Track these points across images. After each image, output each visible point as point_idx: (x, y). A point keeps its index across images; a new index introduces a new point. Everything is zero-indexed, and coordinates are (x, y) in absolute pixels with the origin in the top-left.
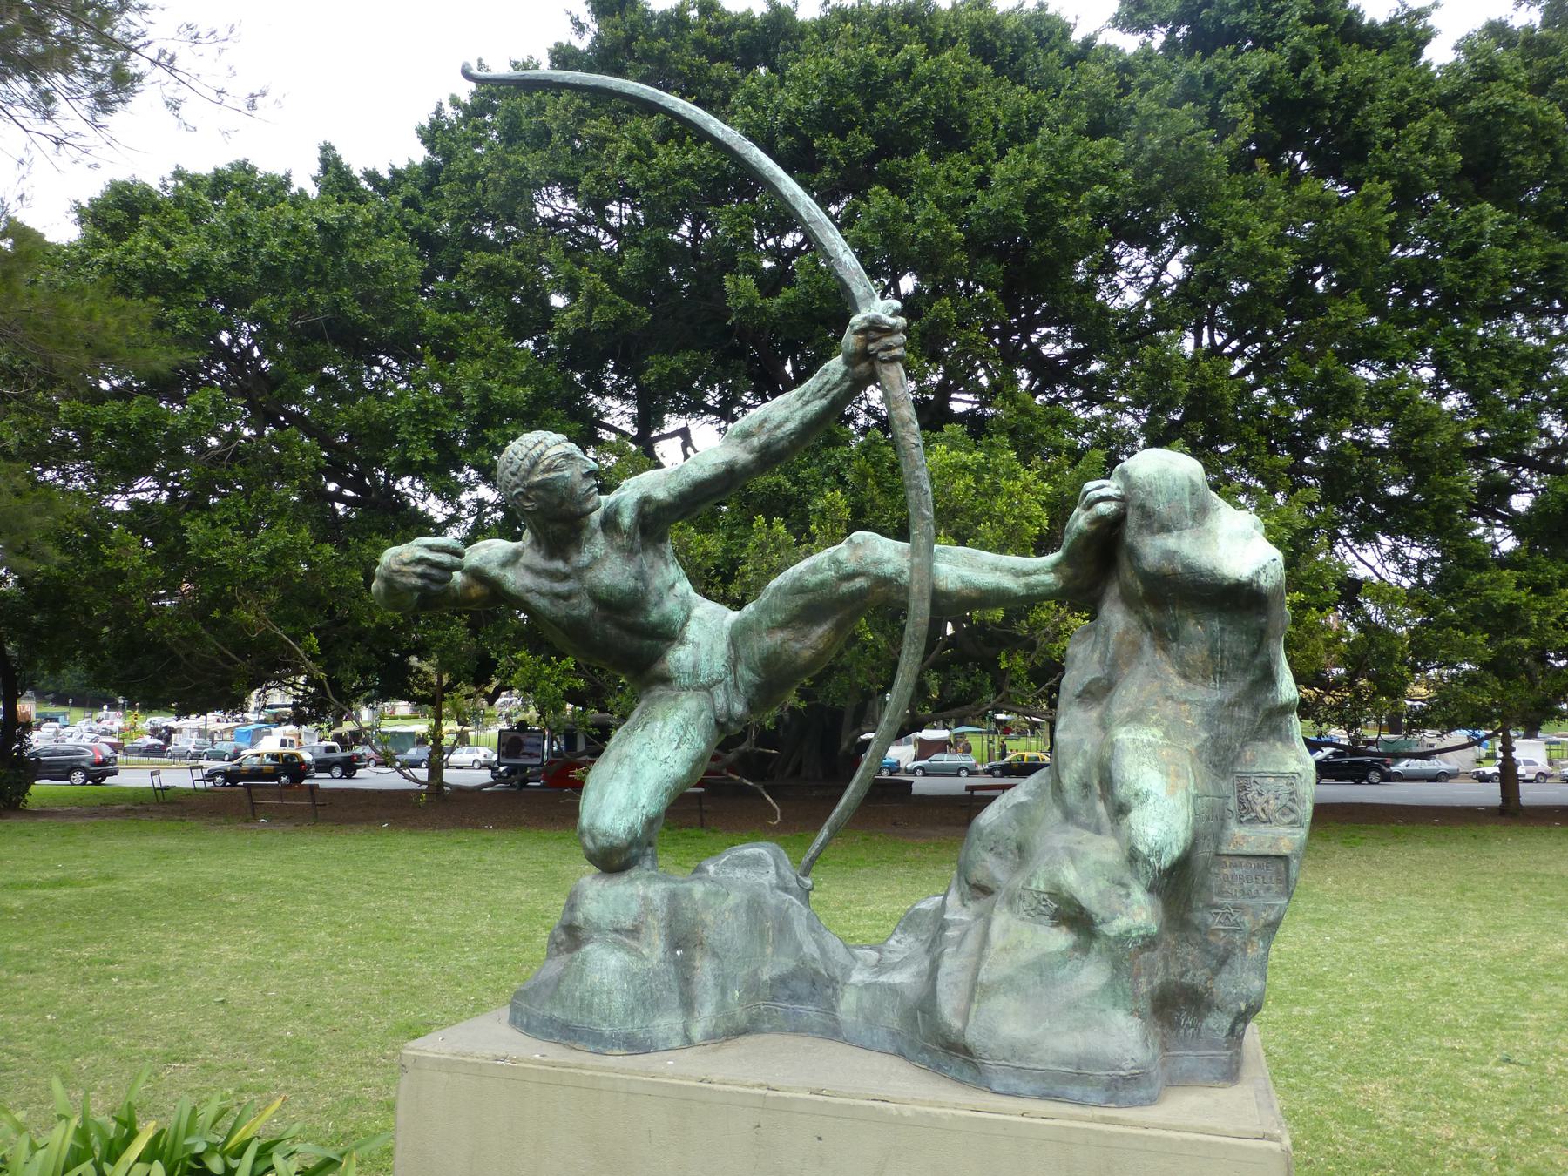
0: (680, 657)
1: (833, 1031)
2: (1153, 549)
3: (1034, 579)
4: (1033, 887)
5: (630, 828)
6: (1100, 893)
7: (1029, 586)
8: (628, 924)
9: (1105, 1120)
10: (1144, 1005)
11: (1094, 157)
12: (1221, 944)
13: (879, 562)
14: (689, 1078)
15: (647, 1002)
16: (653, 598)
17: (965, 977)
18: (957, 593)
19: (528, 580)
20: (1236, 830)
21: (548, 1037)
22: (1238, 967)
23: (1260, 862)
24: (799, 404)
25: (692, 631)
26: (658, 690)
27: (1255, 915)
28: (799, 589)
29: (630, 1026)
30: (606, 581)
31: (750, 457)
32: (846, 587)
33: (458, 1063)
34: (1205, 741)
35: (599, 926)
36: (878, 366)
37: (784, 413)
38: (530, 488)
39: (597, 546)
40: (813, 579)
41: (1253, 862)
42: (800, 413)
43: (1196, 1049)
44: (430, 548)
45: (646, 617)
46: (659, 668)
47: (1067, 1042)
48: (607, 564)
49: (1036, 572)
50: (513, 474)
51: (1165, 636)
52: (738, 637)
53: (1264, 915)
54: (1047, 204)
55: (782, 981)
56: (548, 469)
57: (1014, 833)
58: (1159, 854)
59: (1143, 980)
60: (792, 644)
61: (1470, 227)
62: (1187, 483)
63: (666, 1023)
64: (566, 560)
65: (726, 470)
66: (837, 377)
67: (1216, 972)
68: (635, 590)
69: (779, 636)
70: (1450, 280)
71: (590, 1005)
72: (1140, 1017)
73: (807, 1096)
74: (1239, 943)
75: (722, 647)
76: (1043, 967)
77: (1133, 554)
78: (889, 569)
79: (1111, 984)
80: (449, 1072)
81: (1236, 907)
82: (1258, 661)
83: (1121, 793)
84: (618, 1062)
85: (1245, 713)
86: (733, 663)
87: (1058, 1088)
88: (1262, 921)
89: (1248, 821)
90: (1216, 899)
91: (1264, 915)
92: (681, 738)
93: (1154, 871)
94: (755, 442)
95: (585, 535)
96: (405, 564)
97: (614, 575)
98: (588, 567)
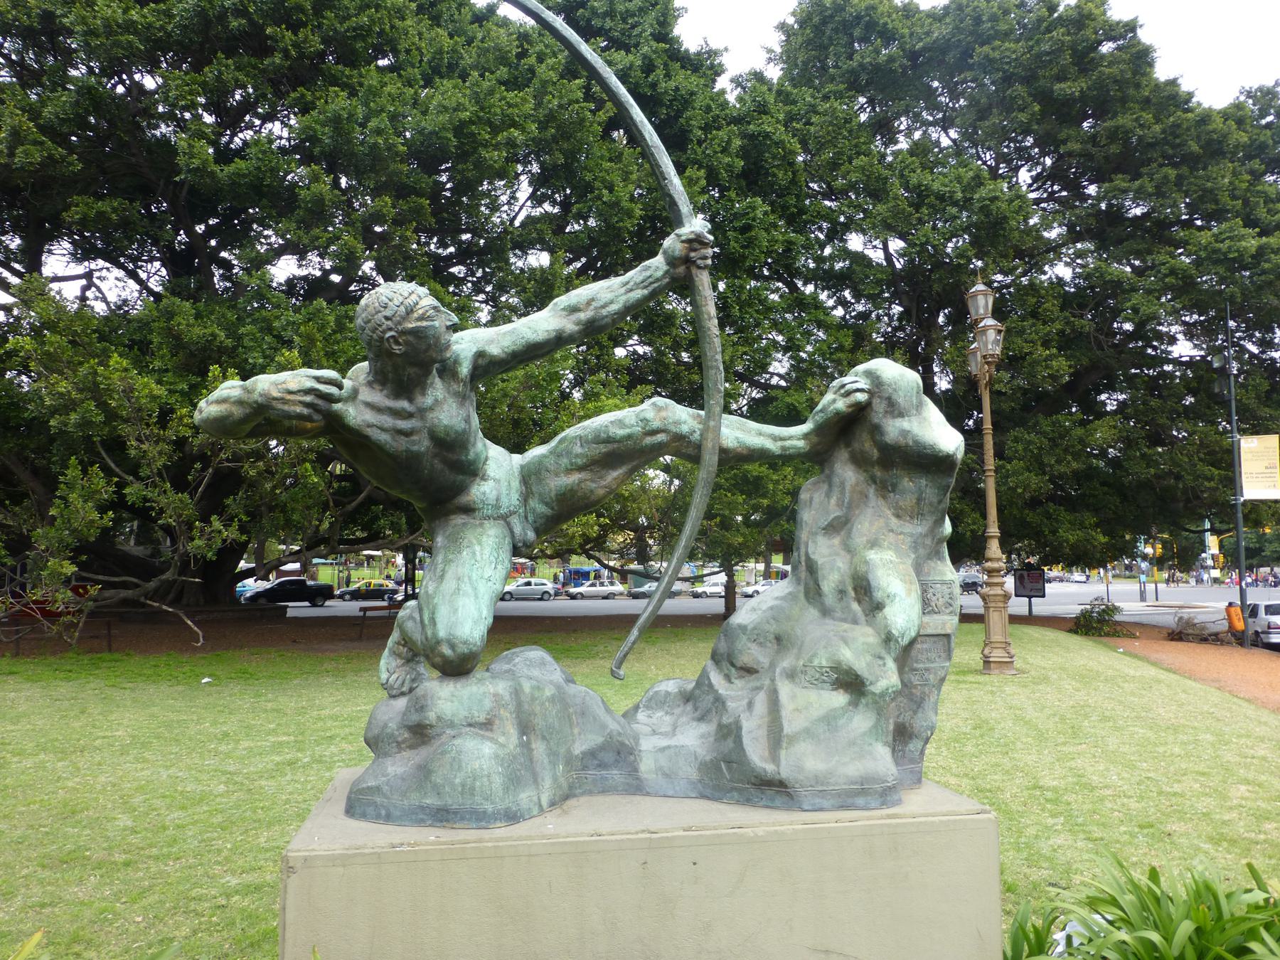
0: (482, 491)
1: (636, 787)
2: (894, 428)
3: (788, 443)
4: (816, 663)
6: (868, 664)
7: (783, 448)
8: (482, 719)
9: (889, 817)
11: (510, 105)
13: (677, 423)
14: (581, 835)
15: (514, 781)
17: (763, 733)
18: (734, 450)
19: (369, 416)
21: (420, 823)
23: (936, 639)
24: (623, 290)
25: (492, 469)
26: (458, 520)
27: (935, 674)
28: (601, 439)
29: (507, 801)
30: (445, 422)
31: (576, 328)
32: (649, 440)
33: (355, 855)
35: (452, 722)
36: (694, 270)
37: (609, 296)
39: (437, 389)
40: (621, 432)
41: (932, 639)
42: (624, 298)
44: (318, 379)
45: (467, 455)
46: (463, 499)
47: (851, 769)
48: (445, 407)
49: (790, 438)
50: (387, 318)
51: (886, 488)
52: (529, 477)
54: (473, 134)
55: (591, 754)
56: (421, 318)
57: (773, 628)
60: (588, 483)
61: (748, 213)
63: (525, 797)
64: (411, 400)
66: (660, 274)
67: (915, 712)
68: (464, 431)
69: (575, 478)
70: (734, 248)
71: (473, 789)
73: (681, 833)
75: (516, 484)
76: (830, 720)
77: (876, 430)
78: (685, 429)
79: (875, 726)
80: (344, 866)
81: (927, 670)
83: (878, 595)
84: (501, 832)
86: (525, 497)
87: (850, 801)
94: (583, 316)
96: (291, 393)
97: (451, 417)
98: (431, 409)
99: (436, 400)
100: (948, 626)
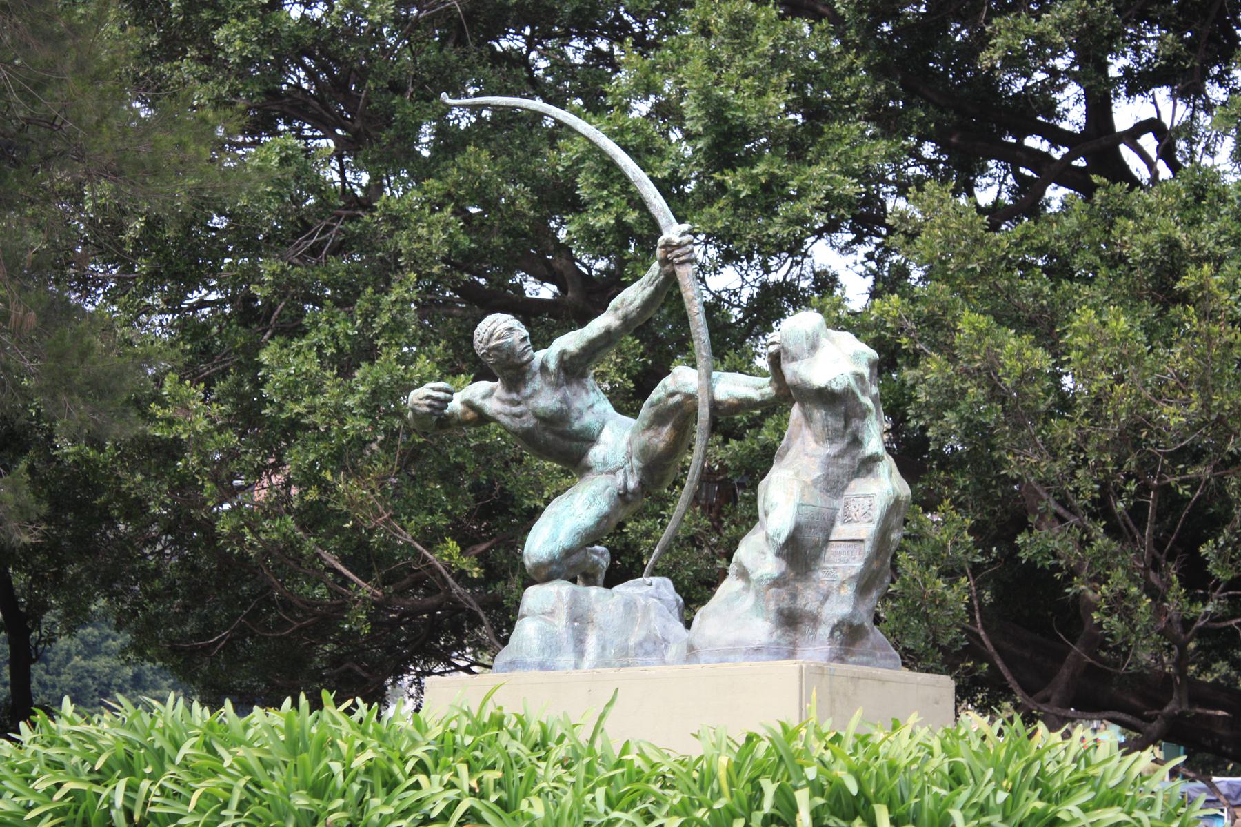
0: (596, 454)
3: (763, 391)
7: (762, 395)
8: (549, 610)
10: (772, 616)
16: (575, 414)
32: (672, 401)
36: (676, 268)
38: (490, 350)
39: (537, 382)
44: (433, 389)
48: (543, 394)
56: (498, 339)
58: (779, 536)
64: (518, 392)
68: (561, 410)
79: (755, 605)
81: (835, 568)
82: (849, 430)
90: (826, 565)
95: (528, 376)
98: (531, 396)
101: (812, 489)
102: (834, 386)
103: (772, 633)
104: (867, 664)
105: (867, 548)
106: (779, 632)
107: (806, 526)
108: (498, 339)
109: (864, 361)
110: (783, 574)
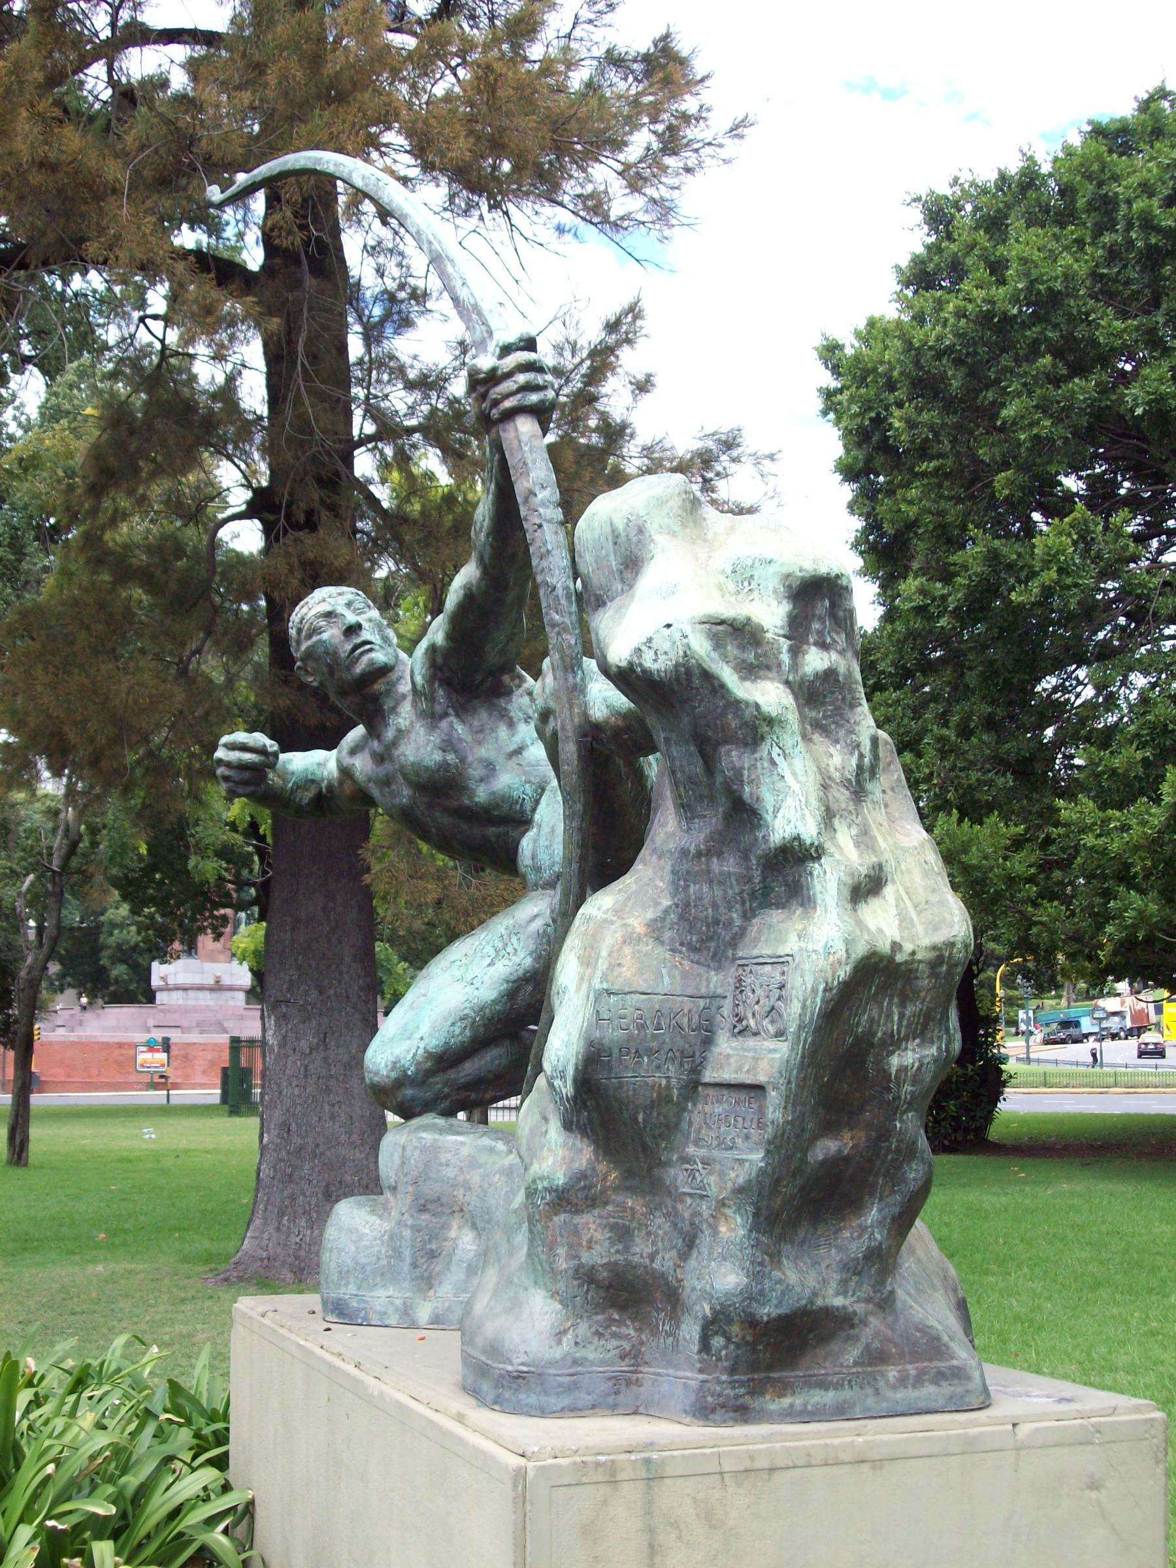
5: (394, 1063)
9: (460, 1418)
12: (686, 1215)
16: (475, 772)
18: (606, 721)
20: (725, 1045)
22: (705, 1251)
23: (743, 1096)
27: (722, 1175)
29: (342, 1291)
30: (411, 759)
34: (666, 912)
41: (734, 1096)
43: (677, 1367)
45: (471, 798)
48: (413, 736)
53: (733, 1175)
59: (561, 1251)
62: (608, 529)
63: (382, 1297)
65: (466, 596)
67: (684, 1256)
68: (444, 766)
72: (561, 1302)
74: (706, 1214)
81: (706, 1162)
82: (719, 779)
85: (730, 865)
88: (729, 1185)
89: (740, 1032)
90: (691, 1150)
91: (733, 1175)
92: (497, 951)
93: (561, 1099)
95: (388, 704)
97: (418, 749)
99: (399, 731)
100: (763, 1065)
101: (648, 946)
102: (648, 661)
103: (560, 1335)
104: (841, 1412)
105: (775, 1109)
106: (583, 1329)
107: (623, 1049)
108: (309, 636)
109: (770, 580)
110: (583, 1175)
